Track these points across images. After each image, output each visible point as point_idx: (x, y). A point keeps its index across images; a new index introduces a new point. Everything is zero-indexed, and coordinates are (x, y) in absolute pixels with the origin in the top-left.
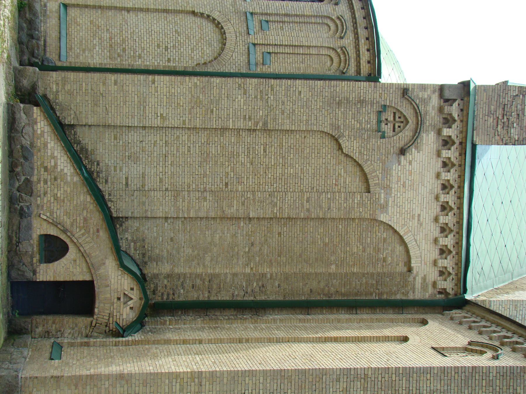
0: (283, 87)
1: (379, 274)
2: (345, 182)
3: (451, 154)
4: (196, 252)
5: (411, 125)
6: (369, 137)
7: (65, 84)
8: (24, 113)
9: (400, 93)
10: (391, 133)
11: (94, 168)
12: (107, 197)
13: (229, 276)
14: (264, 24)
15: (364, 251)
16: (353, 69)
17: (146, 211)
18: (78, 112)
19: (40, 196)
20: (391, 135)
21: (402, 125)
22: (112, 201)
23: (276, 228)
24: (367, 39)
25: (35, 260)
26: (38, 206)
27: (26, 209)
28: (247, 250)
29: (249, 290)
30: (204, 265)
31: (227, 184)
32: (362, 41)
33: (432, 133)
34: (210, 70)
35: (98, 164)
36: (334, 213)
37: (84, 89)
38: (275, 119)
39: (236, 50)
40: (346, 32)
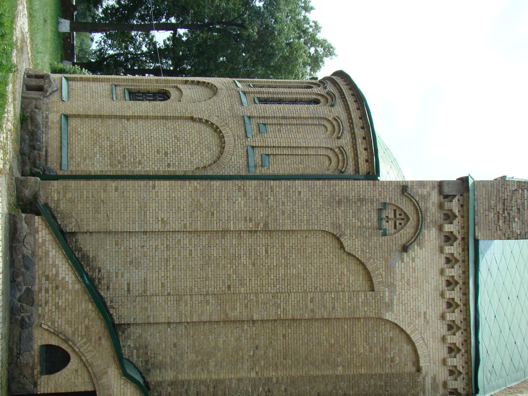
0: (283, 188)
1: (387, 375)
2: (348, 281)
3: (454, 249)
4: (200, 357)
6: (370, 235)
7: (66, 192)
8: (26, 223)
9: (399, 190)
10: (393, 231)
11: (96, 275)
12: (108, 304)
13: (234, 381)
14: (262, 127)
15: (371, 351)
17: (149, 317)
18: (79, 220)
19: (41, 306)
20: (393, 232)
21: (403, 222)
22: (114, 308)
23: (280, 330)
24: (364, 138)
25: (36, 372)
26: (39, 316)
27: (27, 319)
28: (252, 353)
30: (208, 371)
31: (229, 287)
32: (359, 141)
33: (434, 229)
34: (210, 173)
36: (339, 313)
37: (85, 197)
39: (235, 153)
40: (343, 132)
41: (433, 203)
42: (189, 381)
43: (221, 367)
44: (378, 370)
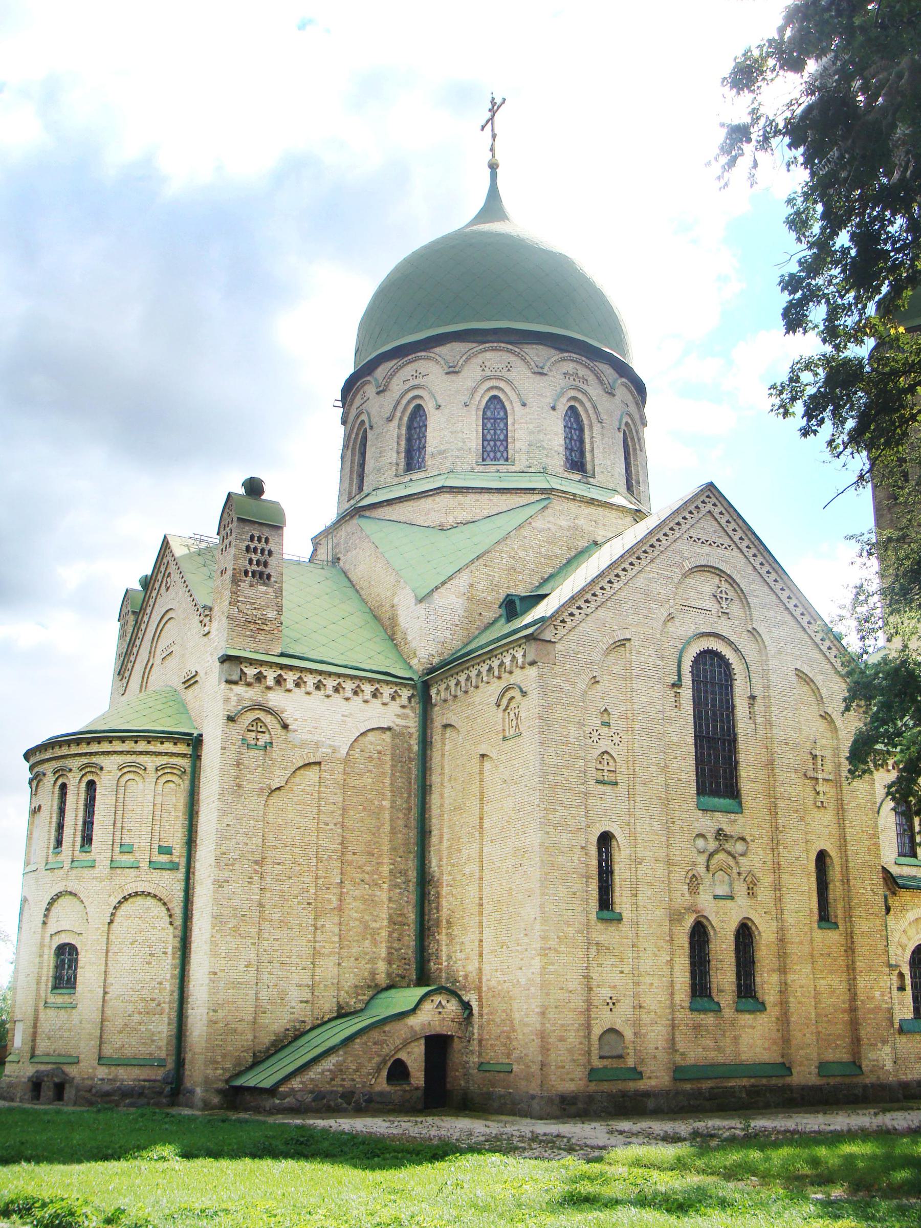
0: (223, 842)
1: (393, 759)
2: (309, 786)
3: (290, 678)
4: (368, 936)
5: (261, 715)
6: (271, 759)
7: (215, 1061)
8: (284, 1099)
9: (231, 724)
10: (267, 736)
11: (291, 1033)
12: (319, 1022)
13: (391, 905)
14: (124, 849)
15: (371, 771)
16: (181, 761)
17: (333, 984)
18: (242, 1049)
19: (355, 1085)
20: (268, 736)
21: (259, 724)
22: (323, 1017)
23: (349, 857)
24: (149, 742)
25: (408, 1088)
26: (364, 1086)
27: (366, 1097)
28: (367, 886)
29: (403, 886)
30: (379, 929)
31: (309, 904)
32: (151, 748)
33: (269, 695)
34: (178, 911)
35: (288, 1030)
36: (339, 799)
37: (221, 1043)
38: (253, 852)
39: (157, 882)
40: (138, 763)
41: (246, 692)
42: (389, 948)
43: (377, 916)
44: (387, 768)
